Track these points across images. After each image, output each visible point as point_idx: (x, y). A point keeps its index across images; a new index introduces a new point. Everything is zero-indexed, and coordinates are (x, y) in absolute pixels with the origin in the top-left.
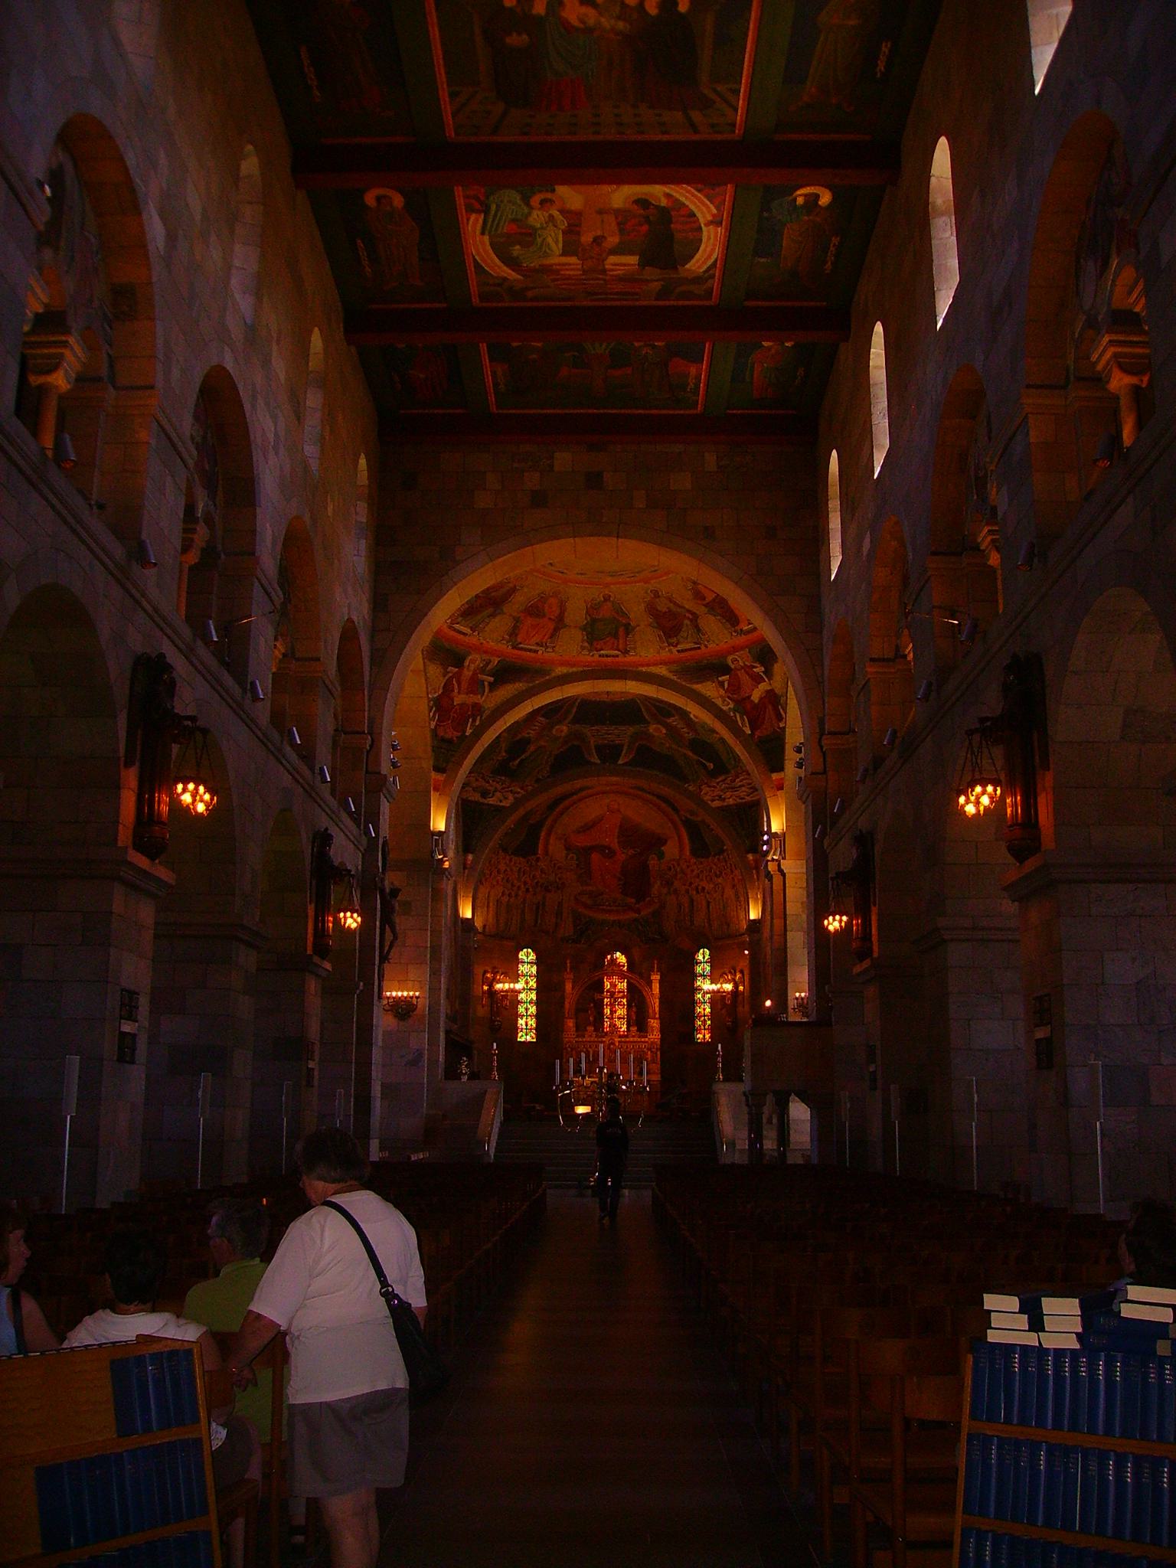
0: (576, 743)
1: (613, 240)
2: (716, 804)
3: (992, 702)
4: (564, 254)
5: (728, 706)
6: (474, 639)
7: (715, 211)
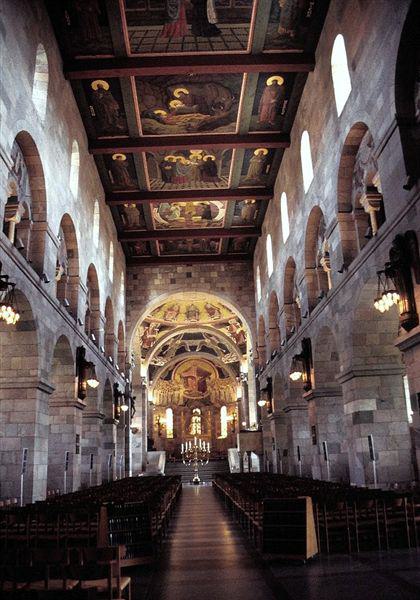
1: (194, 213)
3: (299, 350)
5: (229, 335)
6: (152, 319)
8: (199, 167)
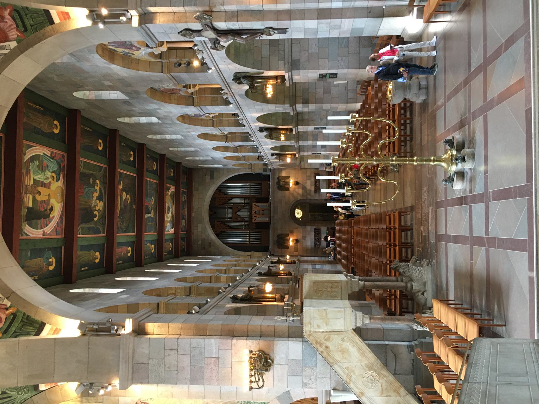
4: (34, 180)
7: (48, 233)
8: (90, 206)
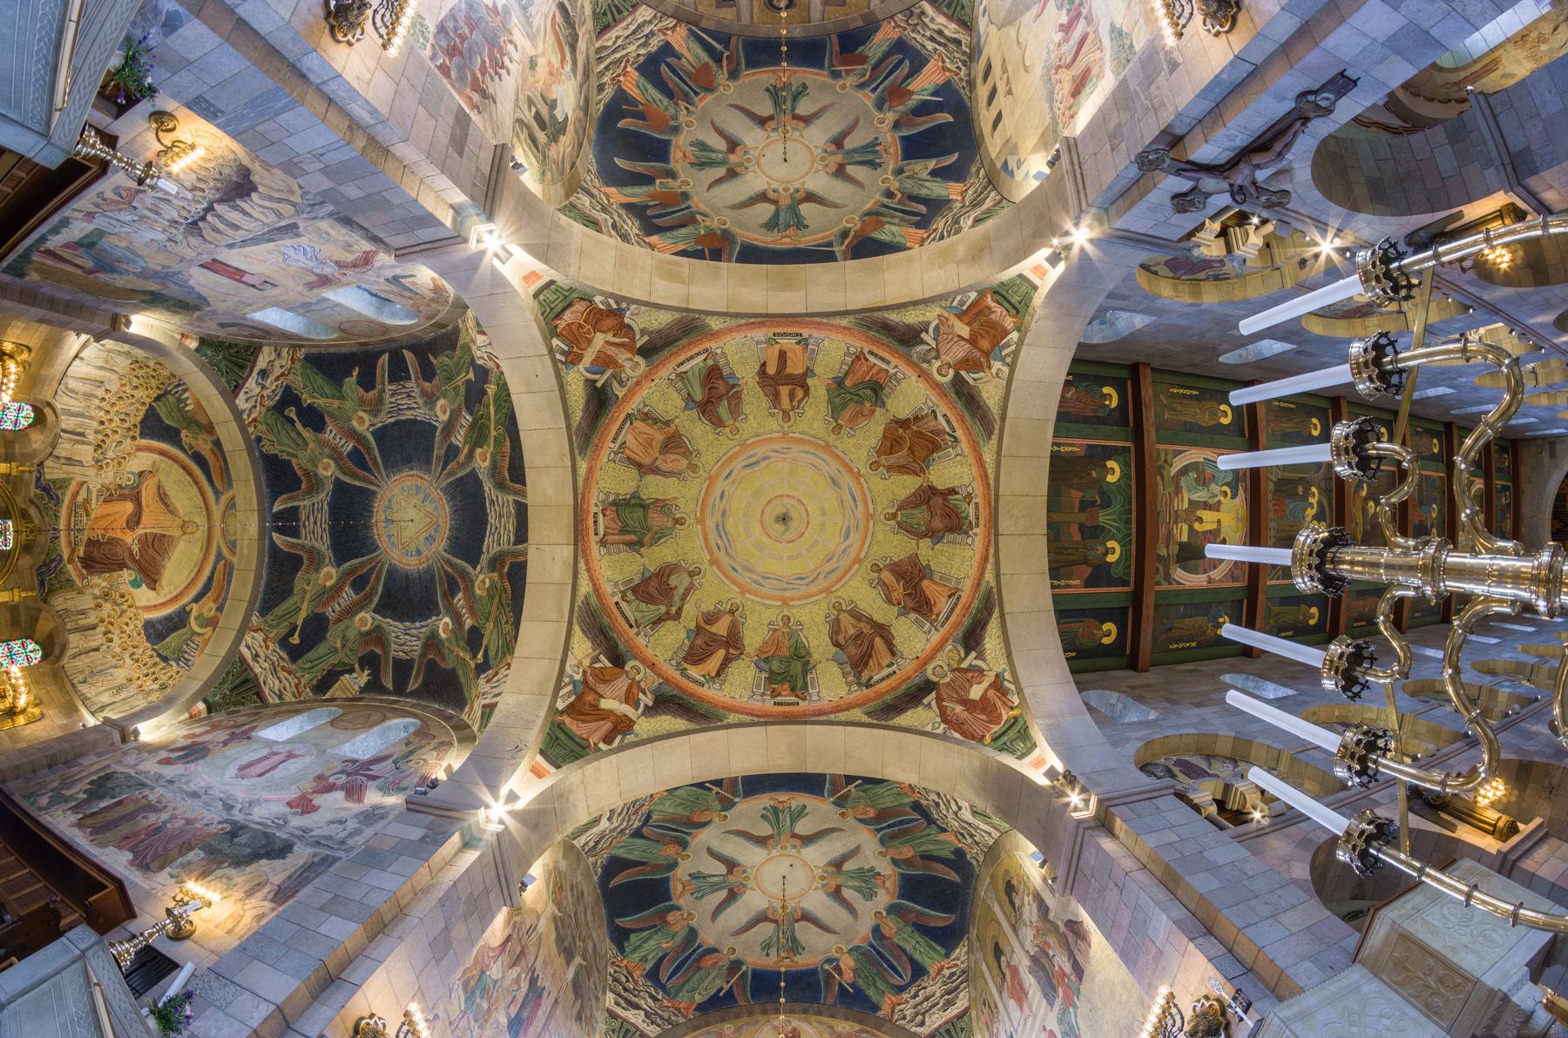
0: (304, 486)
2: (247, 654)
